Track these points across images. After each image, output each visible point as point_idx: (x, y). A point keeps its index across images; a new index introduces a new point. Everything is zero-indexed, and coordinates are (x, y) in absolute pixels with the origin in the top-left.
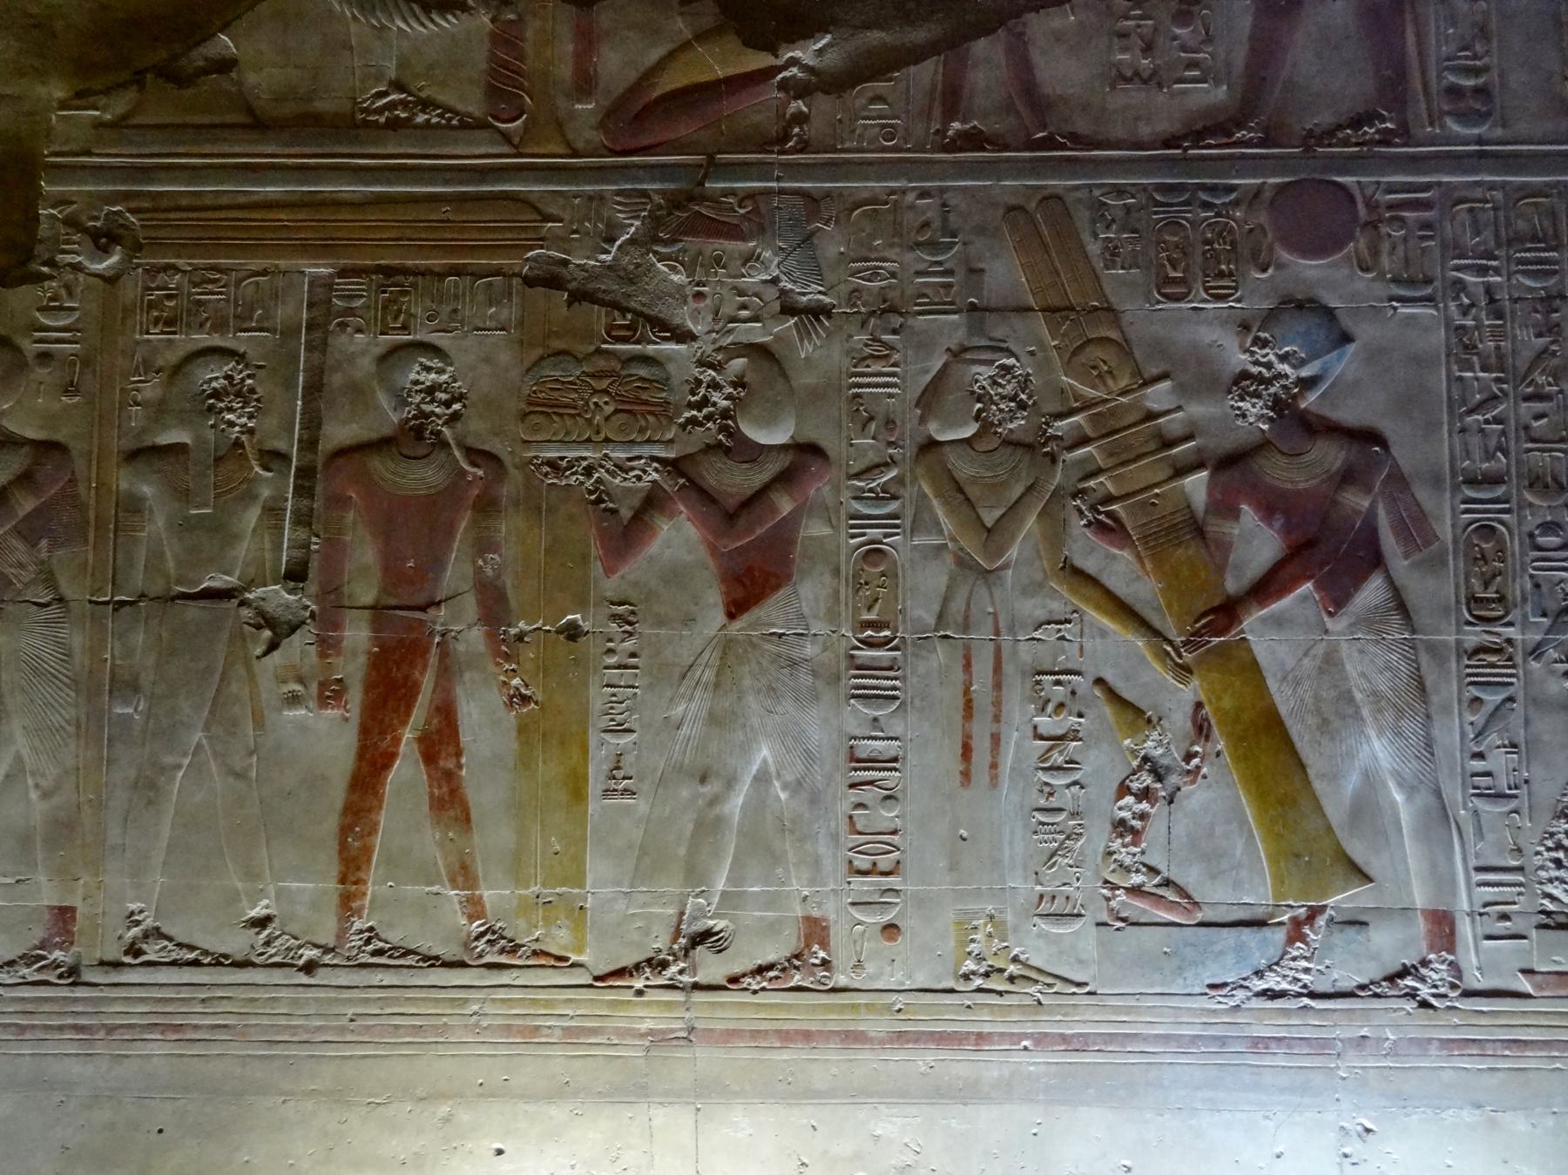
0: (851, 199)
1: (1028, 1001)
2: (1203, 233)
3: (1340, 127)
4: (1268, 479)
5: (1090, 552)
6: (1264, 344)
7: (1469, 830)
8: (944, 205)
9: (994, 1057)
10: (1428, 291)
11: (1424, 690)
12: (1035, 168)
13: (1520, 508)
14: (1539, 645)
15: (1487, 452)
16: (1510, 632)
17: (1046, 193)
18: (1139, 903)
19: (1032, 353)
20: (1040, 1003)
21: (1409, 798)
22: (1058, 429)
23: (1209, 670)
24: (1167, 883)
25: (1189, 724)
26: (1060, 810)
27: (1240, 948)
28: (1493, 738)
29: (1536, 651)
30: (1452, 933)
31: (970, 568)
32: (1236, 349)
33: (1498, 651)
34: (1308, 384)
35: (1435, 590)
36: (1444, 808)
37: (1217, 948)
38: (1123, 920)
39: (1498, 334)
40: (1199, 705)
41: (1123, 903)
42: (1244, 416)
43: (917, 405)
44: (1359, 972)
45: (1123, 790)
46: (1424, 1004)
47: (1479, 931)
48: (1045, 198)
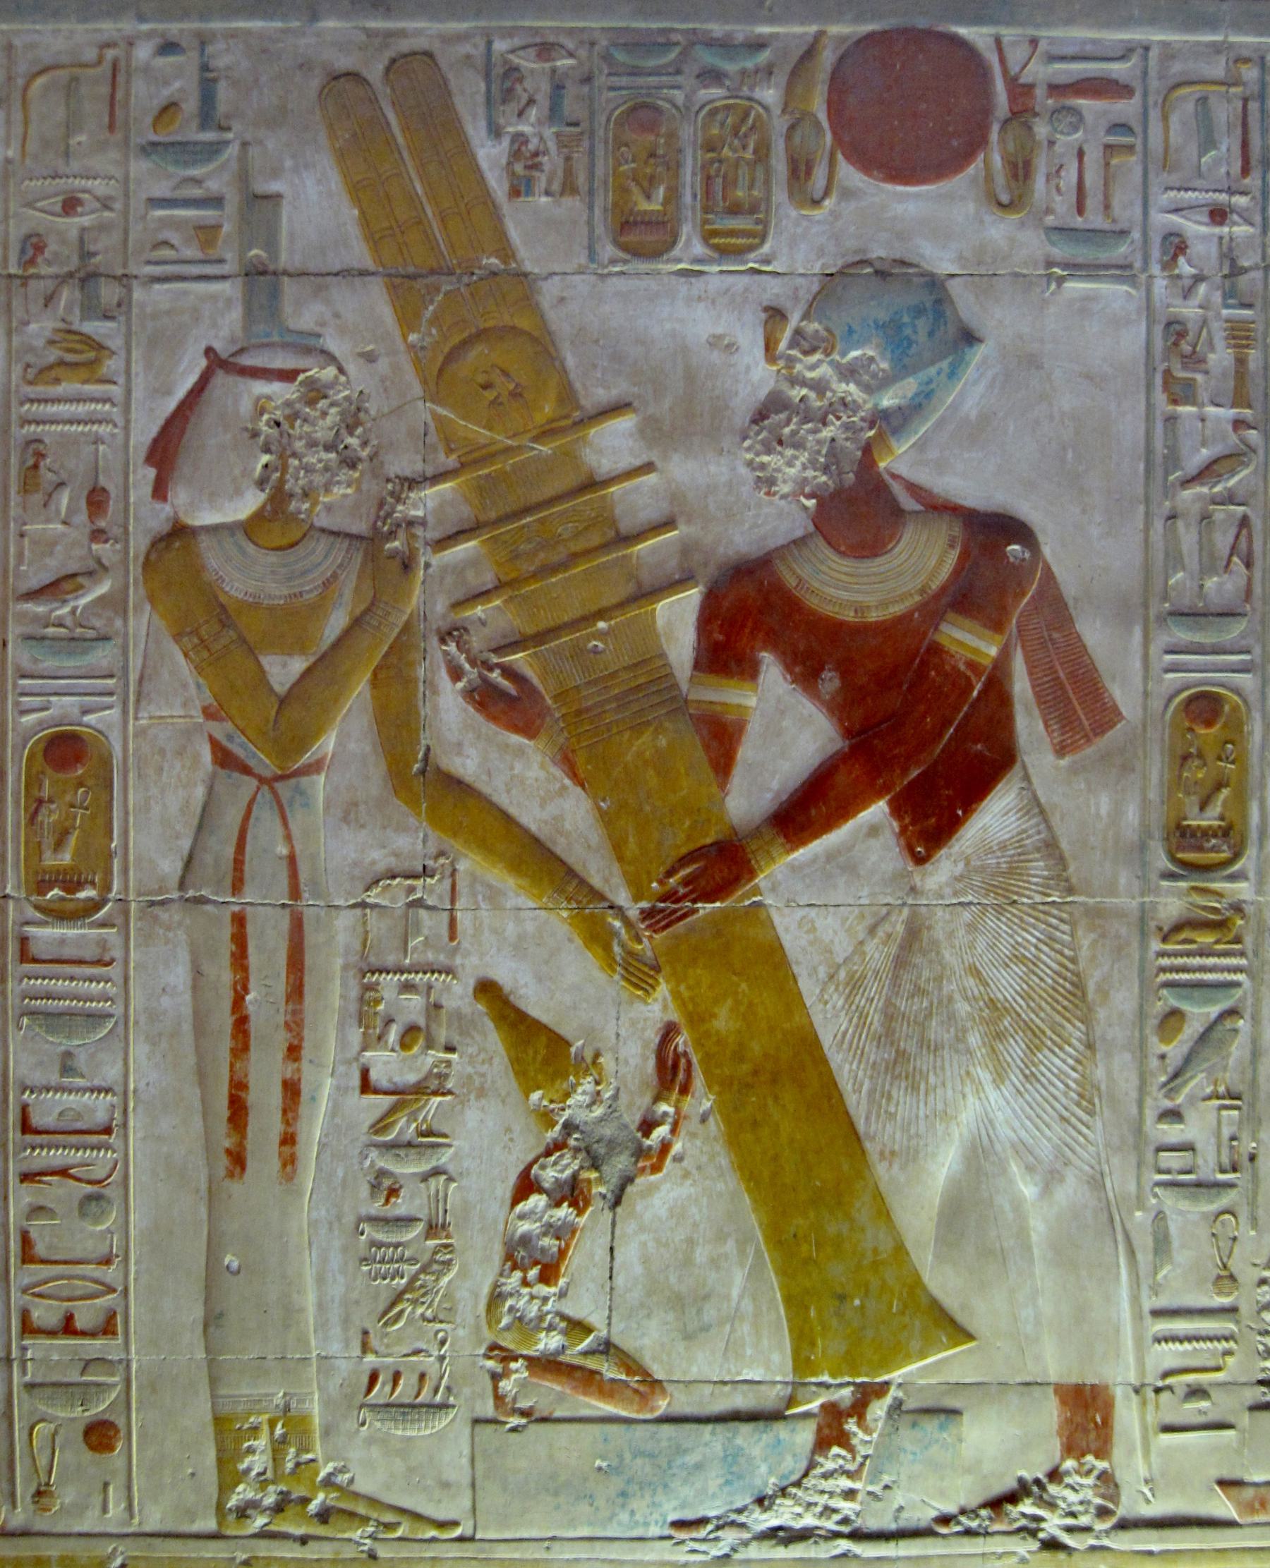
10: (1122, 251)
17: (405, 46)
18: (552, 1386)
20: (372, 1556)
24: (607, 1348)
26: (410, 1220)
27: (733, 1460)
28: (1197, 1082)
30: (1107, 1423)
33: (1220, 925)
34: (889, 423)
37: (691, 1459)
38: (524, 1413)
44: (942, 1494)
45: (526, 1186)
46: (1052, 1545)
47: (1150, 1418)
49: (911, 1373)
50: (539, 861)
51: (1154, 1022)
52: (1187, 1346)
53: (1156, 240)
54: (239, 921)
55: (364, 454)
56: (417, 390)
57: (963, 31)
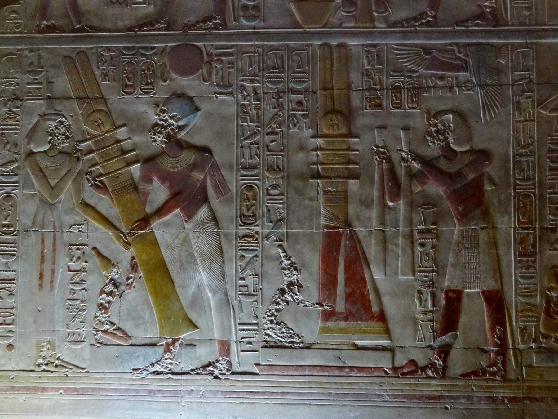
0: (2, 53)
1: (63, 375)
2: (141, 67)
3: (198, 22)
4: (163, 167)
5: (93, 197)
6: (163, 112)
7: (237, 308)
8: (39, 56)
9: (49, 397)
10: (231, 90)
11: (222, 253)
12: (75, 40)
13: (263, 178)
14: (269, 234)
15: (251, 156)
16: (257, 229)
17: (79, 50)
18: (107, 337)
19: (72, 116)
20: (67, 376)
21: (214, 295)
22: (81, 147)
23: (138, 244)
24: (118, 329)
25: (129, 266)
26: (78, 299)
27: (145, 354)
28: (248, 271)
29: (267, 237)
31: (46, 203)
32: (153, 114)
33: (252, 237)
34: (181, 128)
35: (226, 211)
36: (228, 299)
37: (137, 354)
38: (101, 343)
39: (258, 107)
40: (133, 258)
41: (101, 337)
42: (155, 141)
43: (27, 137)
44: (192, 364)
45: (102, 292)
46: (216, 377)
48: (79, 53)
49: (184, 336)
51: (238, 258)
52: (247, 332)
55: (71, 136)
57: (196, 44)
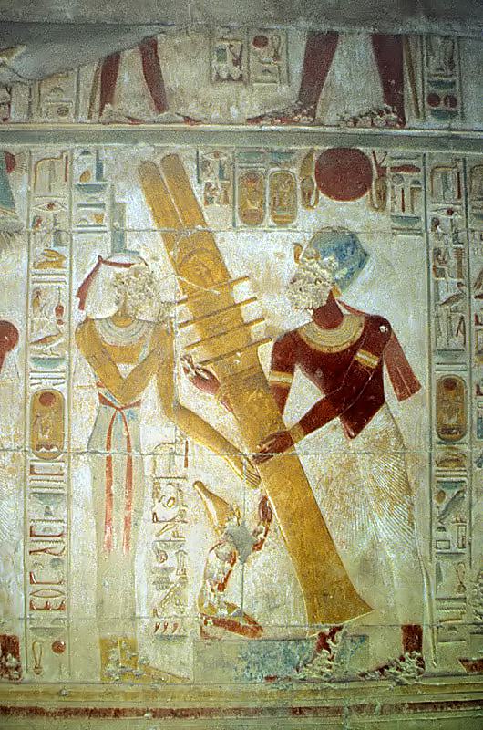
24: (241, 613)
40: (264, 500)
46: (400, 683)
50: (216, 437)
53: (429, 221)
54: (109, 459)
56: (172, 271)
57: (361, 149)
